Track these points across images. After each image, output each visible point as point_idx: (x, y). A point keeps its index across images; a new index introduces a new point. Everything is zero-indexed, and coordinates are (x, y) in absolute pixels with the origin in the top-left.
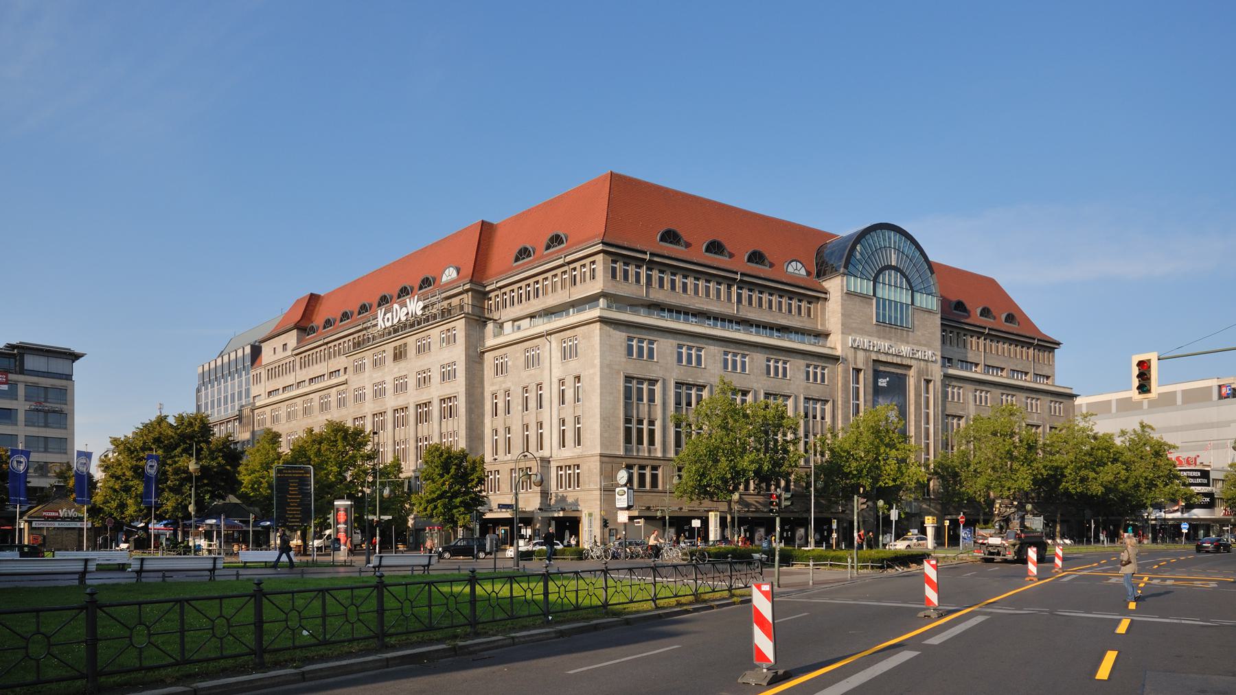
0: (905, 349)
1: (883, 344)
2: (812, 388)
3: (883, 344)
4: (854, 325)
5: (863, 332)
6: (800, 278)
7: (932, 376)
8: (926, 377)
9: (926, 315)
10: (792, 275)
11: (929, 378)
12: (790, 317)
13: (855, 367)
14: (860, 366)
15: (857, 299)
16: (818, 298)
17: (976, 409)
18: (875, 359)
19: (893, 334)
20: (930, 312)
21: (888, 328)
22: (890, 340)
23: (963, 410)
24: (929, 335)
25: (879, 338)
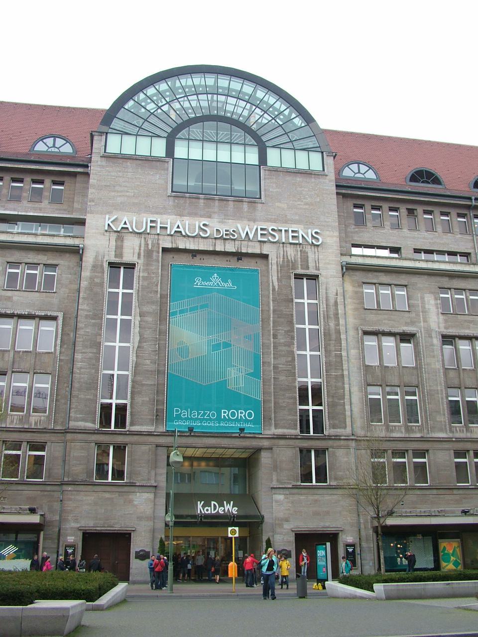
0: (243, 228)
1: (189, 224)
2: (15, 298)
3: (189, 224)
4: (119, 200)
5: (139, 207)
6: (67, 155)
7: (318, 269)
8: (300, 271)
9: (299, 179)
10: (40, 153)
11: (312, 271)
12: (12, 205)
13: (117, 260)
14: (128, 258)
15: (129, 163)
16: (74, 175)
17: (446, 321)
18: (168, 245)
19: (216, 210)
20: (307, 173)
21: (202, 201)
22: (210, 217)
23: (412, 323)
24: (307, 207)
25: (181, 215)
